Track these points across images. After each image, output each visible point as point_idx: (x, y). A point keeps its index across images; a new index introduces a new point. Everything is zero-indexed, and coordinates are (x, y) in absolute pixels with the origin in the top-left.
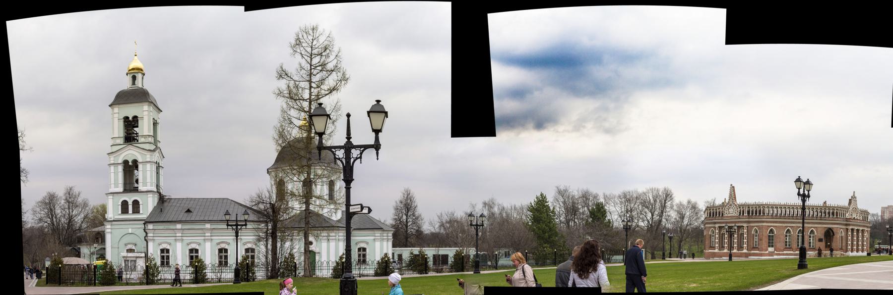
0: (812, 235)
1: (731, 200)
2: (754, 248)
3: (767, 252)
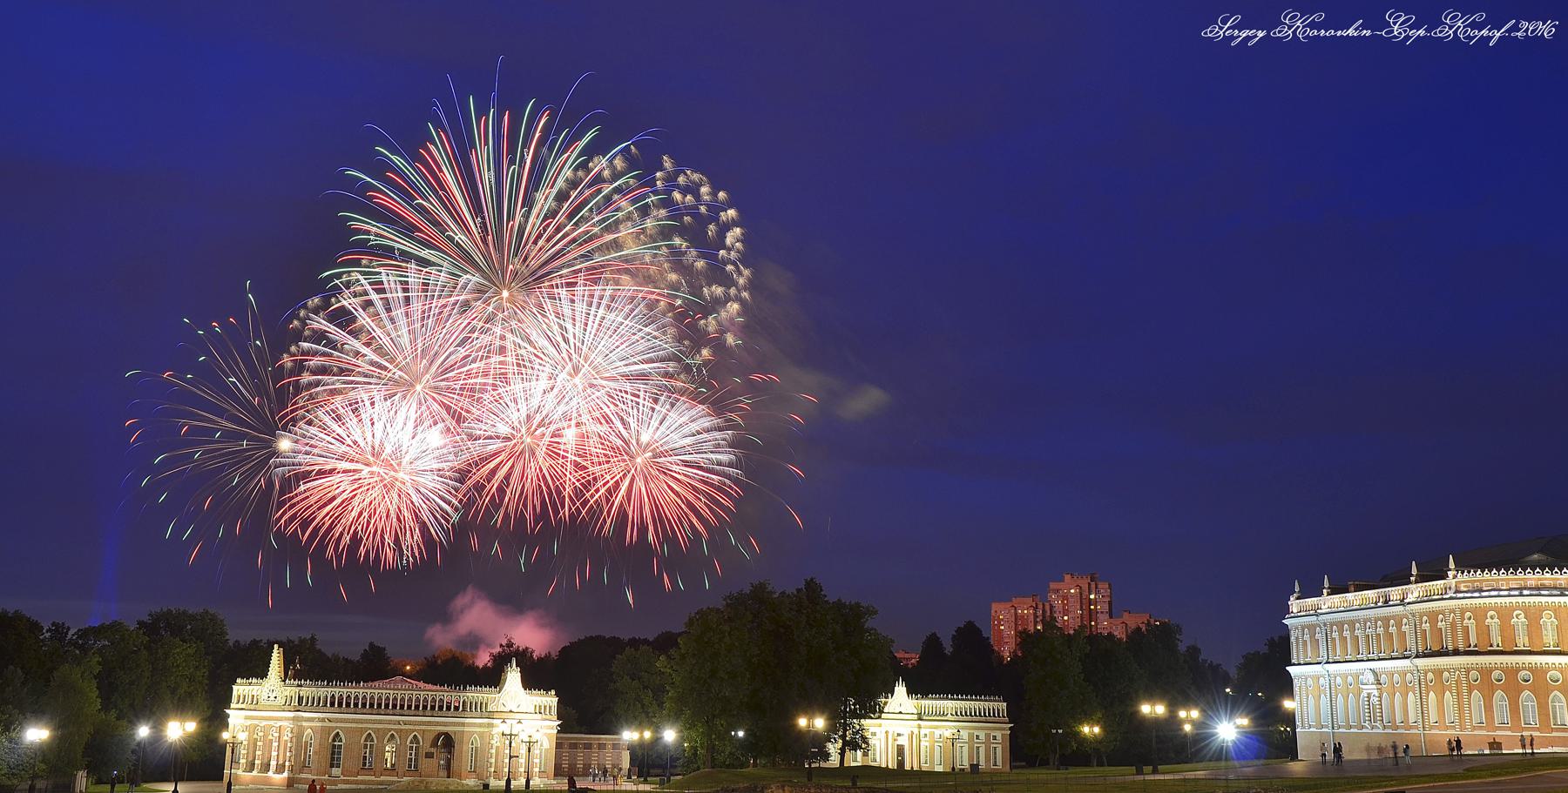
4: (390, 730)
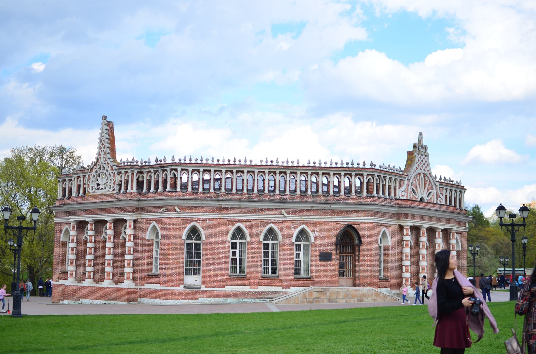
0: (302, 244)
1: (102, 153)
2: (150, 276)
3: (181, 288)
4: (268, 222)
